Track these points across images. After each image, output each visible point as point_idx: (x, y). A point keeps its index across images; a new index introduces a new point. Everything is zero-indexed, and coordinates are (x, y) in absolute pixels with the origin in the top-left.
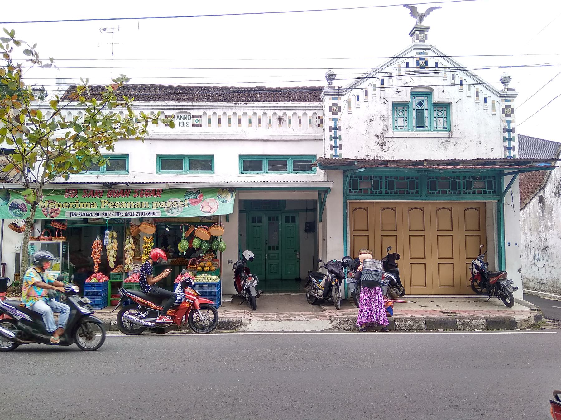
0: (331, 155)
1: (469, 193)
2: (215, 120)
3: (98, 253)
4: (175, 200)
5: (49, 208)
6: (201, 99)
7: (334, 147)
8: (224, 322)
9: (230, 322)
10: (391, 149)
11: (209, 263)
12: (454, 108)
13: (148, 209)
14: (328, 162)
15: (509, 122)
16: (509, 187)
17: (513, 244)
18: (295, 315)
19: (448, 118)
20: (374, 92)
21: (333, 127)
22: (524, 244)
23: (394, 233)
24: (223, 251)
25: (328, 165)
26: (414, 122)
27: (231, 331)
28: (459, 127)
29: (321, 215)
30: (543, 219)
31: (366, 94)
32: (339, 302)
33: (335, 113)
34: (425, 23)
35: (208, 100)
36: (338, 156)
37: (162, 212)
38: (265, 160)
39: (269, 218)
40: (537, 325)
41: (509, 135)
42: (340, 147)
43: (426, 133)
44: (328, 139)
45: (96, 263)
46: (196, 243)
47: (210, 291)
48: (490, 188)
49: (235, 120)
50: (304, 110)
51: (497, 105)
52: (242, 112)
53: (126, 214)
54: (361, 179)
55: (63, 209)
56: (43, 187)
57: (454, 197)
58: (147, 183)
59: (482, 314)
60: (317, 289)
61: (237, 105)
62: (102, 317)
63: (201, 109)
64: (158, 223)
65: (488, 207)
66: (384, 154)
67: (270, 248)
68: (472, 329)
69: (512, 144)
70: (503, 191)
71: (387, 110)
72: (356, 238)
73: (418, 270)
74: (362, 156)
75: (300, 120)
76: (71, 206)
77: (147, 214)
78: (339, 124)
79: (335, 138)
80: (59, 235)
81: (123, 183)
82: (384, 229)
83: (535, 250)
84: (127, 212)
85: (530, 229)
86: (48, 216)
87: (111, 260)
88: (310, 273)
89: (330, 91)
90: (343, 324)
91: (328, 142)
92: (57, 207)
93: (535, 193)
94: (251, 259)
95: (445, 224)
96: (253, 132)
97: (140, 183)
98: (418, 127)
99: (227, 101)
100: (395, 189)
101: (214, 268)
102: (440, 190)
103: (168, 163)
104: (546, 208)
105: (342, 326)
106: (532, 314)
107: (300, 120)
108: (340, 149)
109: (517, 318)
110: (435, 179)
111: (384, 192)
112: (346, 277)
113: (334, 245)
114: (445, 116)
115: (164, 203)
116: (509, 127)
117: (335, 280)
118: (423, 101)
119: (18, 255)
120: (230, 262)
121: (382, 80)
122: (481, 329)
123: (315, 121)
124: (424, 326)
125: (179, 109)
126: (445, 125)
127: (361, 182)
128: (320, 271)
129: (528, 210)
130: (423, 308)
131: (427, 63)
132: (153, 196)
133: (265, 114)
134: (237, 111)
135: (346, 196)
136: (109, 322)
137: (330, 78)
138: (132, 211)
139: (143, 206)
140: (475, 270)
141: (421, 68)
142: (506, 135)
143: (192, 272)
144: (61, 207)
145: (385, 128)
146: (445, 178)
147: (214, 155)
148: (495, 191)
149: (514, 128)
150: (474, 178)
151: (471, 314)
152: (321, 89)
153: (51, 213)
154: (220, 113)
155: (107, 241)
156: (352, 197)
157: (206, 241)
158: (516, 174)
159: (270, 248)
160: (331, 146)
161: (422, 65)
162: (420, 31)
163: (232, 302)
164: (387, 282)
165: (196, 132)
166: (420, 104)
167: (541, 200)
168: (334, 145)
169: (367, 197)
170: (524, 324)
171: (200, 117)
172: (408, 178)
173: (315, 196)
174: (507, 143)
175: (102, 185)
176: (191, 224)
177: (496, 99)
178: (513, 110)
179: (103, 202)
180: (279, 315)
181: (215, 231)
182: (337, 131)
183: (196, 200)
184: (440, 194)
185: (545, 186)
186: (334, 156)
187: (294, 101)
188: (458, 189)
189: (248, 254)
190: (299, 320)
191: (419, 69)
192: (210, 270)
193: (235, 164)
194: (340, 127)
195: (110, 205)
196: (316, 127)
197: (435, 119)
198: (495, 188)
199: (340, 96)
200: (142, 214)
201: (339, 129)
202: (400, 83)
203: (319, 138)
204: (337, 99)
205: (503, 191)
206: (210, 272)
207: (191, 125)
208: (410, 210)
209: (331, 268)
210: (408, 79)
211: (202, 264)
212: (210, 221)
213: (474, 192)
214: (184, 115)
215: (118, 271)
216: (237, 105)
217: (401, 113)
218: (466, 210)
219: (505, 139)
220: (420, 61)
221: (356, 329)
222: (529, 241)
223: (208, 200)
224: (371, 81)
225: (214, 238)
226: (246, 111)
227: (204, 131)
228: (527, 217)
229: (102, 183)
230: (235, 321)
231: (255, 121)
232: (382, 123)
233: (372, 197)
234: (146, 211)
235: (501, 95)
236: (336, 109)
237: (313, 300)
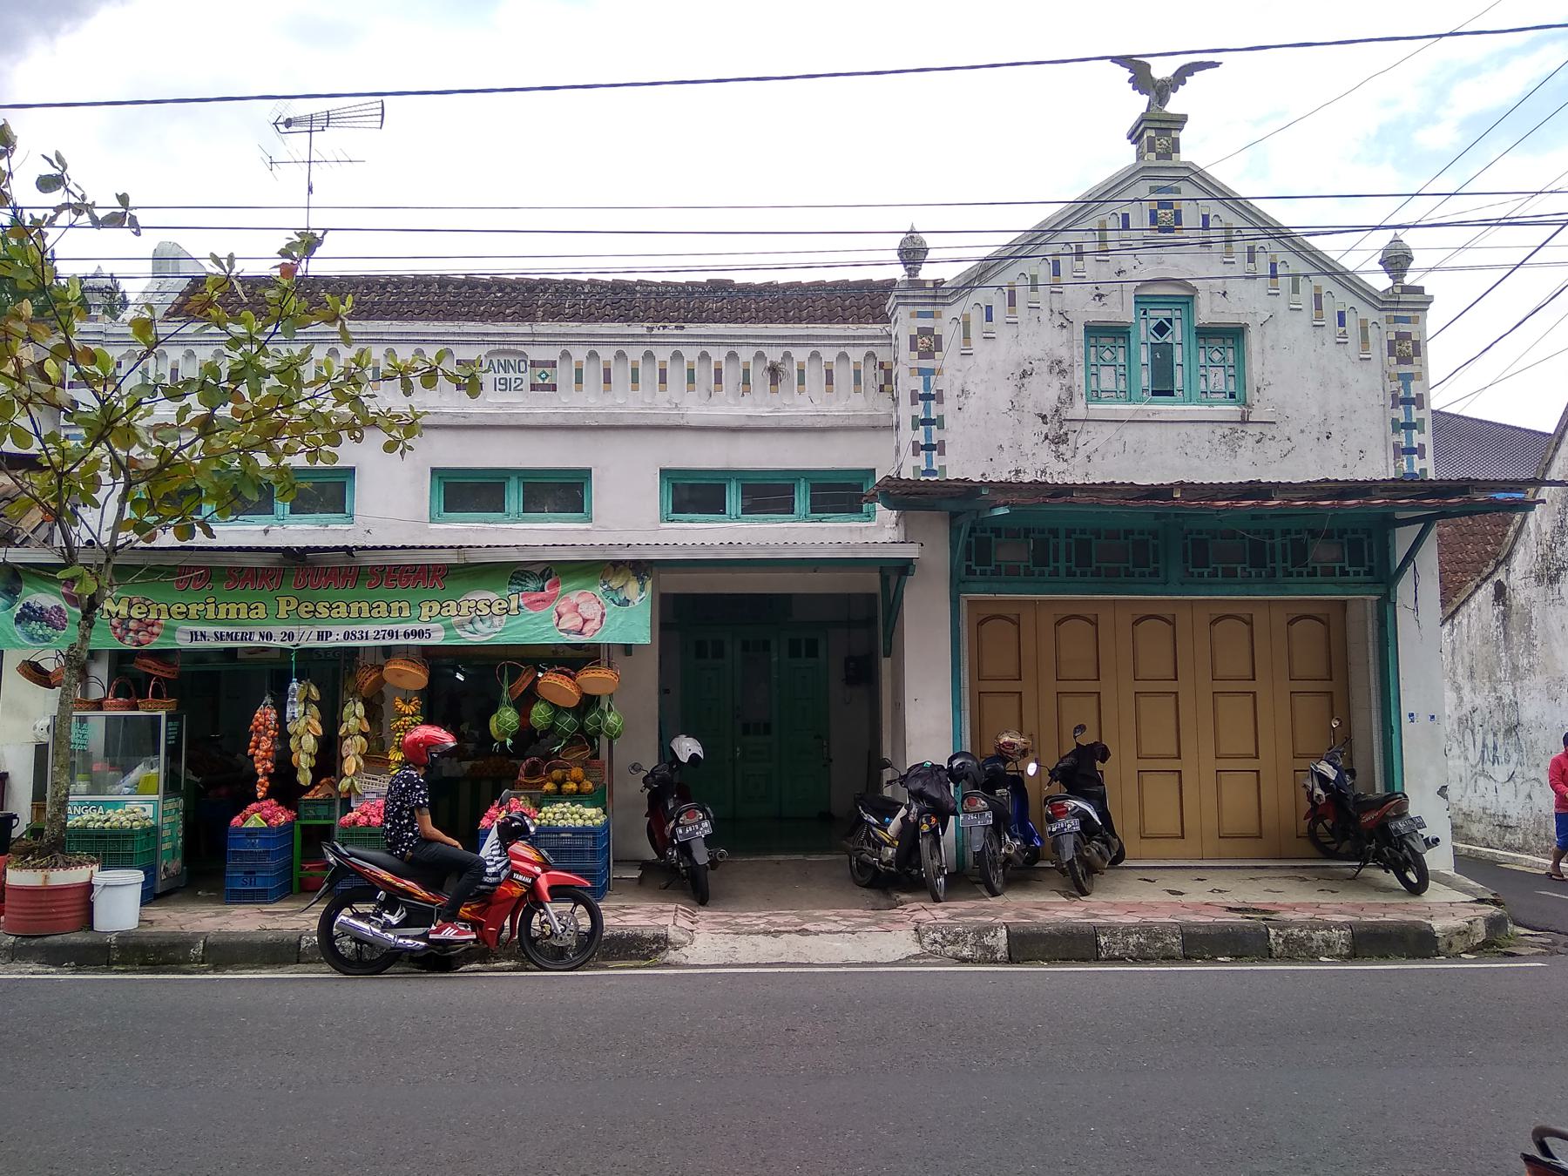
0: (916, 468)
1: (1300, 574)
2: (592, 375)
3: (266, 744)
4: (482, 596)
5: (131, 618)
6: (554, 315)
7: (923, 447)
8: (620, 937)
10: (1082, 453)
11: (577, 772)
12: (1253, 340)
13: (407, 620)
14: (905, 490)
15: (1406, 378)
17: (1422, 719)
18: (818, 919)
19: (1239, 370)
21: (921, 392)
22: (1455, 716)
24: (617, 736)
25: (908, 497)
26: (1145, 379)
27: (637, 963)
28: (1269, 393)
29: (889, 636)
30: (1507, 649)
31: (1012, 303)
32: (941, 880)
33: (927, 354)
34: (1174, 106)
35: (574, 317)
36: (934, 473)
37: (446, 629)
38: (734, 484)
39: (745, 646)
40: (1493, 943)
42: (940, 448)
44: (906, 424)
45: (260, 771)
46: (540, 714)
47: (580, 852)
48: (1357, 559)
49: (648, 374)
50: (839, 345)
52: (670, 350)
53: (347, 636)
55: (172, 623)
56: (116, 561)
57: (1258, 587)
58: (403, 547)
59: (1340, 912)
60: (881, 843)
61: (655, 331)
62: (276, 925)
63: (555, 344)
64: (436, 659)
65: (1353, 612)
66: (1063, 466)
67: (746, 729)
68: (1313, 957)
69: (1417, 438)
70: (1393, 570)
71: (1071, 346)
73: (1160, 792)
74: (1002, 474)
75: (829, 373)
76: (193, 609)
77: (406, 635)
78: (937, 384)
79: (927, 422)
80: (157, 694)
81: (337, 549)
83: (1485, 734)
84: (350, 629)
85: (1472, 676)
86: (128, 640)
87: (304, 763)
88: (860, 799)
89: (910, 293)
90: (953, 943)
91: (907, 435)
92: (153, 616)
94: (694, 757)
96: (697, 409)
97: (384, 548)
98: (1155, 393)
99: (628, 319)
100: (1095, 565)
101: (590, 786)
103: (465, 491)
104: (1514, 617)
106: (1479, 912)
107: (829, 373)
108: (942, 453)
109: (1437, 925)
110: (1204, 536)
111: (1062, 571)
112: (959, 810)
113: (927, 726)
114: (1231, 362)
115: (453, 604)
116: (1408, 391)
117: (928, 821)
118: (1169, 321)
119: (41, 750)
120: (636, 768)
121: (1056, 264)
122: (1339, 956)
123: (870, 375)
124: (1178, 949)
125: (494, 343)
126: (1232, 388)
128: (887, 792)
129: (1465, 621)
130: (1174, 898)
131: (1178, 214)
132: (421, 586)
133: (732, 356)
134: (653, 349)
135: (958, 583)
136: (294, 939)
137: (912, 253)
138: (364, 628)
139: (395, 614)
140: (1319, 791)
141: (1161, 230)
142: (1400, 414)
143: (530, 796)
144: (164, 616)
145: (1063, 397)
146: (1232, 535)
147: (587, 473)
148: (1371, 568)
149: (1420, 396)
150: (1314, 534)
151: (1308, 915)
152: (889, 285)
153: (137, 632)
154: (607, 354)
155: (294, 709)
156: (974, 586)
157: (567, 709)
158: (1428, 522)
159: (746, 729)
160: (915, 443)
161: (1166, 223)
162: (1157, 131)
163: (641, 880)
164: (1073, 825)
165: (542, 407)
166: (1161, 329)
167: (1500, 592)
170: (1456, 940)
171: (554, 364)
172: (1129, 532)
173: (871, 583)
174: (1401, 438)
175: (279, 555)
176: (525, 661)
177: (1372, 315)
179: (283, 601)
180: (774, 919)
181: (595, 679)
183: (540, 595)
184: (1220, 579)
185: (1509, 555)
186: (925, 473)
187: (812, 319)
189: (687, 747)
190: (829, 932)
192: (578, 792)
193: (651, 496)
195: (302, 609)
196: (873, 392)
197: (1203, 371)
198: (1371, 560)
199: (940, 308)
200: (391, 634)
201: (939, 397)
202: (1107, 272)
203: (882, 423)
204: (931, 315)
205: (1393, 570)
206: (578, 797)
208: (1136, 623)
209: (918, 785)
210: (1127, 261)
211: (557, 774)
212: (580, 653)
213: (1313, 573)
214: (509, 357)
215: (320, 796)
216: (655, 331)
217: (1107, 355)
218: (1291, 623)
219: (1397, 426)
221: (989, 957)
222: (1467, 707)
223: (574, 598)
224: (1027, 266)
225: (589, 702)
227: (567, 403)
228: (1461, 642)
229: (278, 549)
230: (648, 934)
231: (704, 375)
232: (1056, 382)
234: (401, 628)
236: (928, 344)
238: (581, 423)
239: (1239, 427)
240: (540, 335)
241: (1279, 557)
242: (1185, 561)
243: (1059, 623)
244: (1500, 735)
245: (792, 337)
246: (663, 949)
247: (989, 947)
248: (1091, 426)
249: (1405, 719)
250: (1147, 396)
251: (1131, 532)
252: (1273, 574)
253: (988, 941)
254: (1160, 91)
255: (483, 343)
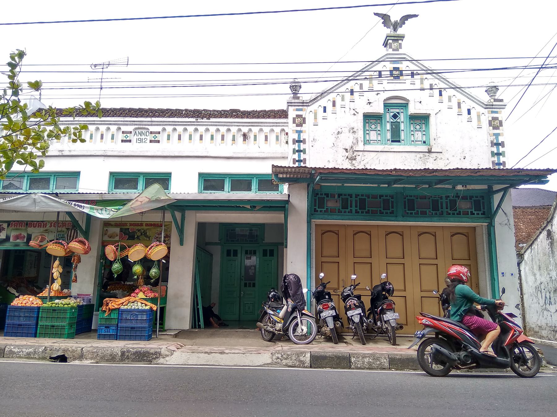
8: (140, 352)
9: (148, 352)
12: (432, 120)
15: (497, 135)
16: (499, 206)
17: (508, 275)
19: (426, 133)
20: (343, 103)
21: (297, 139)
22: (534, 286)
23: (368, 260)
26: (389, 136)
30: (553, 257)
31: (334, 105)
33: (300, 125)
38: (228, 179)
41: (498, 149)
43: (401, 147)
48: (478, 208)
50: (271, 126)
51: (482, 117)
52: (205, 127)
54: (328, 197)
57: (435, 218)
60: (274, 323)
61: (199, 120)
63: (160, 125)
65: (478, 231)
70: (493, 212)
72: (324, 264)
79: (299, 151)
82: (356, 255)
83: (546, 292)
90: (286, 359)
93: (542, 228)
95: (428, 251)
98: (392, 141)
100: (367, 209)
102: (419, 210)
104: (555, 244)
105: (284, 362)
111: (354, 211)
114: (424, 129)
116: (497, 140)
118: (398, 113)
124: (387, 365)
125: (137, 125)
127: (327, 201)
129: (536, 247)
136: (3, 347)
142: (495, 149)
145: (354, 142)
147: (171, 174)
148: (484, 212)
149: (503, 142)
154: (180, 129)
161: (396, 74)
162: (394, 40)
165: (153, 149)
166: (395, 116)
168: (297, 159)
169: (335, 217)
171: (159, 133)
172: (381, 196)
174: (495, 159)
177: (482, 110)
178: (501, 123)
182: (302, 144)
185: (552, 218)
188: (440, 210)
190: (234, 353)
191: (392, 78)
194: (304, 140)
197: (412, 133)
198: (484, 209)
199: (305, 107)
201: (304, 141)
204: (301, 110)
207: (148, 141)
213: (459, 214)
214: (141, 130)
216: (199, 120)
218: (452, 236)
219: (493, 154)
220: (394, 72)
222: (539, 282)
226: (208, 127)
230: (152, 351)
231: (218, 137)
232: (351, 136)
233: (339, 217)
235: (487, 106)
236: (300, 121)
237: (269, 336)
238: (168, 155)
239: (427, 154)
240: (154, 122)
241: (444, 205)
242: (405, 208)
243: (355, 234)
244: (552, 293)
245: (252, 123)
246: (157, 358)
247: (301, 361)
248: (366, 153)
249: (500, 275)
250: (389, 142)
251: (383, 196)
252: (442, 213)
253: (302, 358)
254: (396, 26)
255: (132, 125)
